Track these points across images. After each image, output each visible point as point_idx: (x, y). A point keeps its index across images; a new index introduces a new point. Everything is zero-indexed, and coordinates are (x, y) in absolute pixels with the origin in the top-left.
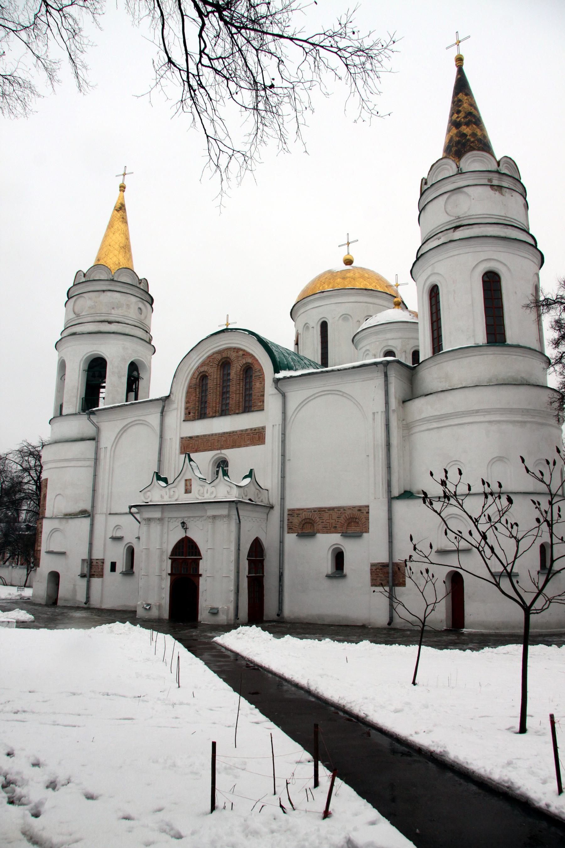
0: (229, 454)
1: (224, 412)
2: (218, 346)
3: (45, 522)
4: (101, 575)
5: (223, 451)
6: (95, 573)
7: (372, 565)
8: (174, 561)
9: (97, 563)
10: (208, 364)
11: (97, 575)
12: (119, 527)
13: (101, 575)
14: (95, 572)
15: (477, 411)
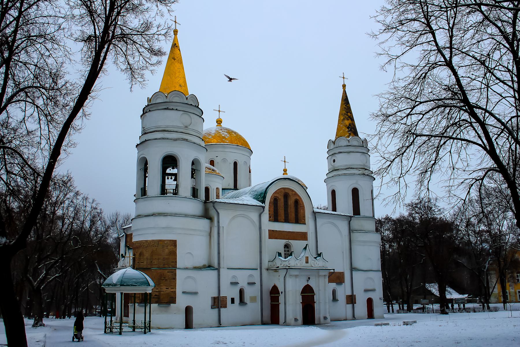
0: (293, 243)
1: (287, 220)
2: (284, 186)
3: (178, 272)
4: (225, 307)
5: (290, 241)
6: (221, 305)
7: (347, 296)
8: (303, 297)
9: (223, 299)
10: (278, 193)
11: (224, 306)
12: (235, 277)
13: (225, 307)
14: (222, 304)
15: (375, 242)
